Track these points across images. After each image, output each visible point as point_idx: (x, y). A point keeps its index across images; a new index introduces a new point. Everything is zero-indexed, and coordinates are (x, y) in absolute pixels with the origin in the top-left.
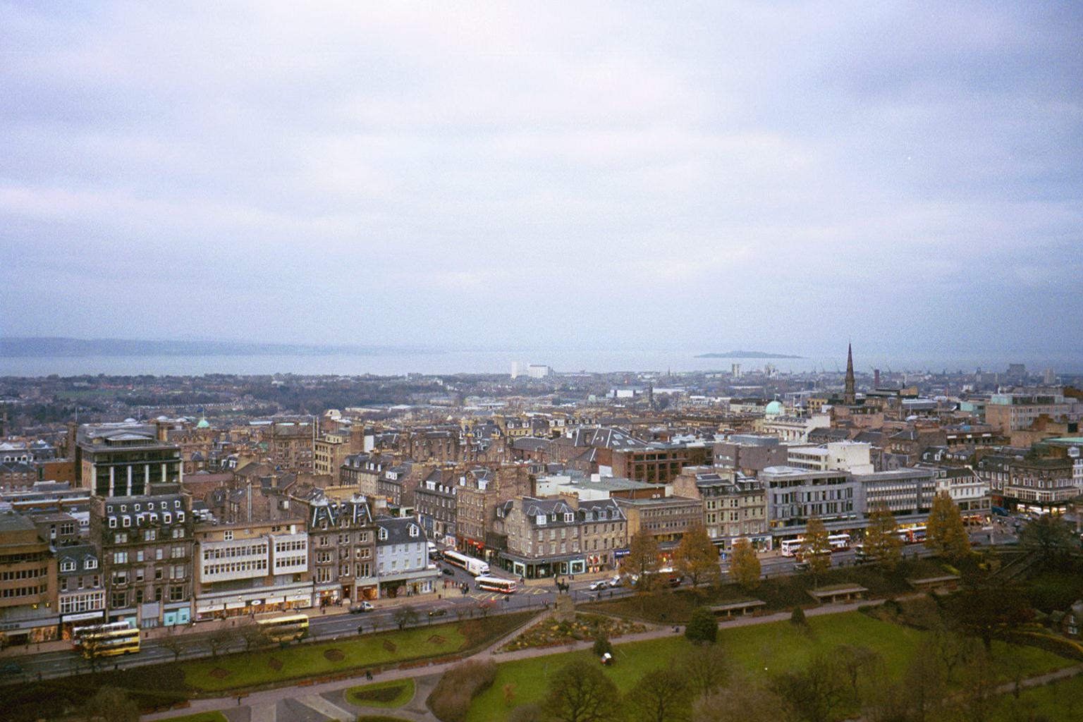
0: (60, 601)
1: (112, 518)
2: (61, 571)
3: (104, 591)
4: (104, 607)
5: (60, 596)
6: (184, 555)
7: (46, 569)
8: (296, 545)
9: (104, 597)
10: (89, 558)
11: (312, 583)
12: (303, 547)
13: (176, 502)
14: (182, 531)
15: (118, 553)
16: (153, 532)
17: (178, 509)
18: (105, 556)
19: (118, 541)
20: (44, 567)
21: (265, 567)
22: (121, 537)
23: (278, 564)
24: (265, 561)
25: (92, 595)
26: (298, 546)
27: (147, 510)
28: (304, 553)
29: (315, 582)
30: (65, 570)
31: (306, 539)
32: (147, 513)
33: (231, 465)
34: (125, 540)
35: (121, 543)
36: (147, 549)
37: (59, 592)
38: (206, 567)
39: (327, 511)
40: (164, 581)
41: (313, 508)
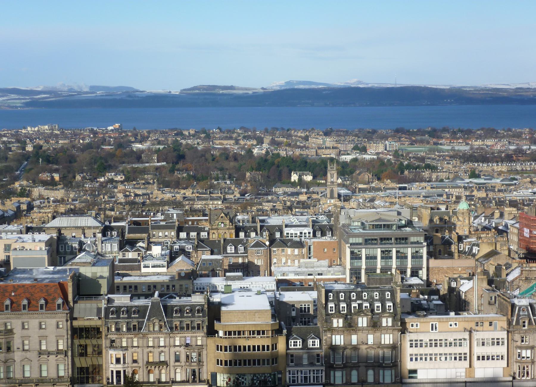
0: (288, 373)
1: (331, 305)
2: (290, 347)
3: (324, 368)
4: (324, 381)
5: (288, 369)
6: (391, 343)
7: (276, 345)
8: (496, 341)
9: (324, 373)
10: (313, 338)
11: (511, 379)
12: (503, 344)
13: (387, 293)
14: (390, 320)
15: (335, 335)
16: (365, 319)
17: (388, 300)
18: (324, 338)
19: (335, 325)
20: (274, 343)
21: (465, 359)
22: (338, 322)
23: (478, 358)
24: (465, 354)
25: (314, 371)
26: (497, 342)
27: (362, 299)
28: (502, 350)
29: (514, 378)
30: (292, 347)
31: (505, 337)
32: (359, 302)
33: (474, 251)
34: (341, 325)
35: (338, 327)
36: (360, 333)
37: (288, 366)
38: (411, 355)
39: (528, 310)
40: (375, 364)
41: (513, 306)
